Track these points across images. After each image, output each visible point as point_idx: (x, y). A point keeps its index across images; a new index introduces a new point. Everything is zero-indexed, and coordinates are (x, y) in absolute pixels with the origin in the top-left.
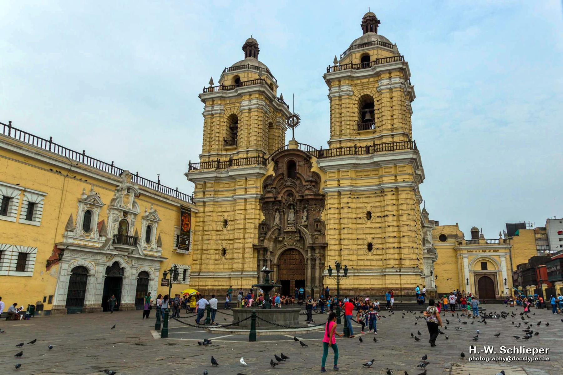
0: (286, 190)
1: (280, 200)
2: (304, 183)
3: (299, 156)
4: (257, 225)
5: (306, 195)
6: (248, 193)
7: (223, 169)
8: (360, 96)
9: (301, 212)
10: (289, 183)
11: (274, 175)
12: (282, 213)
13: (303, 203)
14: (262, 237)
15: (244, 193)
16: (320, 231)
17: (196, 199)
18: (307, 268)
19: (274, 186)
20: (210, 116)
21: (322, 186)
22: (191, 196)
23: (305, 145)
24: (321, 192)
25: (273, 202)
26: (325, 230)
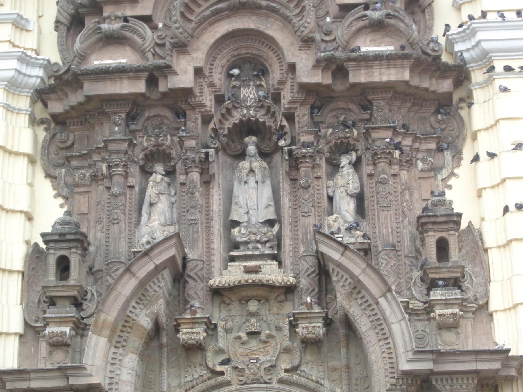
12: (195, 176)
13: (329, 119)
14: (62, 321)
26: (488, 280)
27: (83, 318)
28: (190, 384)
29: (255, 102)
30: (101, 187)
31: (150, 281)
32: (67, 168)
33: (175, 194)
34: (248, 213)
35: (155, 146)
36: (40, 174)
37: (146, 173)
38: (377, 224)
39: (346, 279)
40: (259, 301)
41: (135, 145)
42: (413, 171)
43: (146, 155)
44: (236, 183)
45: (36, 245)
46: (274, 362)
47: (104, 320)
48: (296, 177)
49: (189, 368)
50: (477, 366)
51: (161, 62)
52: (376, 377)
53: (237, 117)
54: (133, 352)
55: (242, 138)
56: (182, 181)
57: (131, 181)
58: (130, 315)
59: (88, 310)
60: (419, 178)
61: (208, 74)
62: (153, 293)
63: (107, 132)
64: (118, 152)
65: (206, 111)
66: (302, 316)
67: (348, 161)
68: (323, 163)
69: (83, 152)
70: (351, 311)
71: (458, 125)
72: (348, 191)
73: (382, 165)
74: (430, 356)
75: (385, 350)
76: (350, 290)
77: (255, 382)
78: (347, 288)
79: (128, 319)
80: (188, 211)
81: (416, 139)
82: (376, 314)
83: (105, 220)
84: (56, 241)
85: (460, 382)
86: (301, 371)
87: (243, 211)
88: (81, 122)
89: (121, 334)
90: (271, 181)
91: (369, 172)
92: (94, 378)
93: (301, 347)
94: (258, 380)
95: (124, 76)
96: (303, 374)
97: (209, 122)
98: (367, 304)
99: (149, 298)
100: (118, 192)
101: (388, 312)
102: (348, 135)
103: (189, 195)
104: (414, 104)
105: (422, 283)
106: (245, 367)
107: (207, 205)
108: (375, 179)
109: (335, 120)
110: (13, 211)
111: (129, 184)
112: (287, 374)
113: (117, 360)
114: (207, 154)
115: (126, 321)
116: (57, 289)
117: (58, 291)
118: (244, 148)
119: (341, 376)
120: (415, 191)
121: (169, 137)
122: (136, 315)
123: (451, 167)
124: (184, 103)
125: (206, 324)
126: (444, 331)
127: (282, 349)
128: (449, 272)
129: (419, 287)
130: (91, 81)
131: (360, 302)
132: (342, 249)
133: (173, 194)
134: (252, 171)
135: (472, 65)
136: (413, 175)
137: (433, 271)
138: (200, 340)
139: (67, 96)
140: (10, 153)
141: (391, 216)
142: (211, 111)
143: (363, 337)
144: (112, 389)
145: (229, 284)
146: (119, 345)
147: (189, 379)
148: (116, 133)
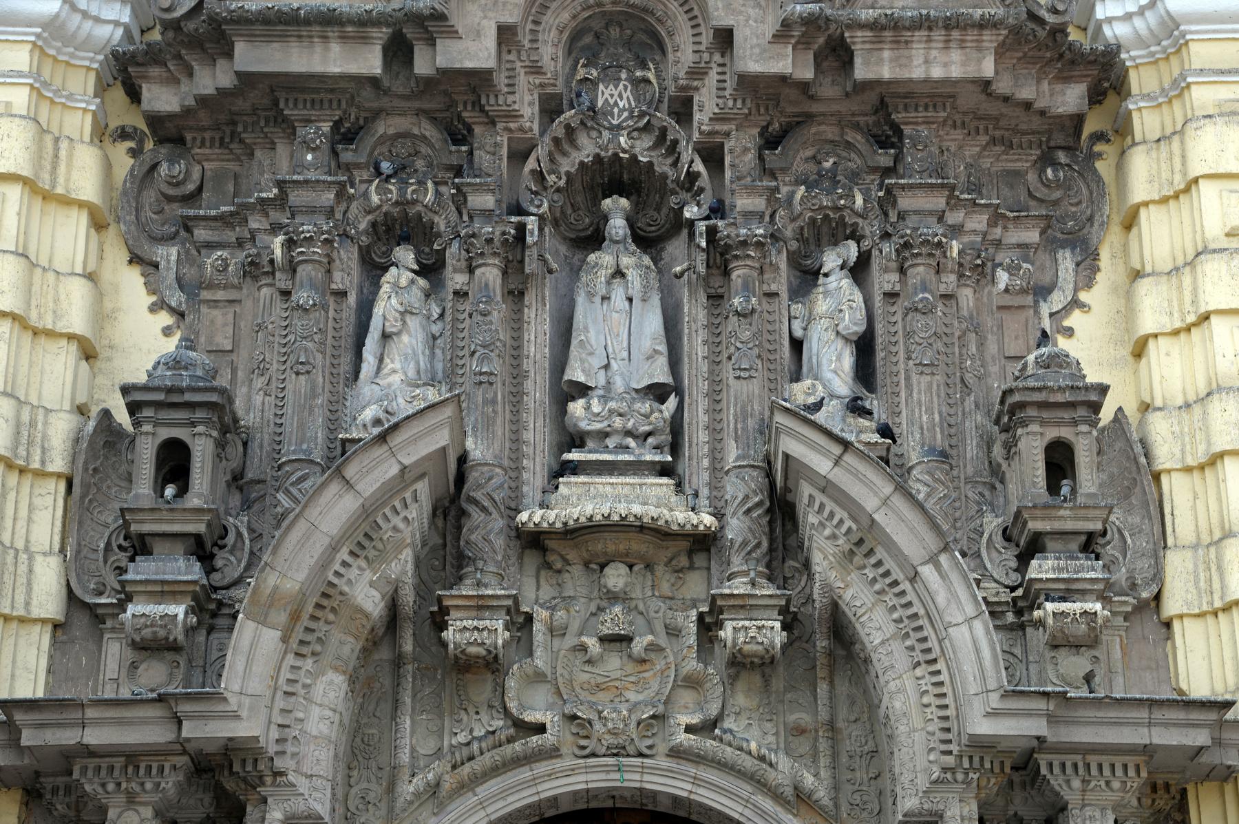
12: (490, 274)
13: (800, 165)
14: (165, 591)
27: (215, 589)
28: (465, 752)
29: (631, 117)
30: (265, 290)
31: (384, 504)
32: (183, 244)
33: (442, 316)
34: (607, 367)
35: (397, 203)
36: (117, 255)
38: (903, 406)
39: (841, 521)
40: (631, 567)
41: (351, 198)
42: (986, 291)
43: (374, 225)
44: (581, 299)
45: (106, 414)
46: (661, 708)
47: (276, 588)
48: (720, 291)
49: (463, 712)
50: (1150, 736)
52: (904, 750)
53: (587, 149)
54: (336, 669)
55: (596, 202)
56: (458, 287)
57: (340, 280)
58: (335, 581)
59: (226, 570)
60: (1000, 308)
61: (527, 45)
62: (390, 533)
63: (284, 164)
64: (312, 210)
65: (521, 129)
66: (732, 602)
67: (840, 262)
68: (782, 262)
69: (224, 209)
70: (848, 595)
71: (1091, 193)
72: (840, 328)
73: (919, 272)
74: (1041, 704)
75: (930, 688)
76: (847, 547)
77: (615, 751)
78: (840, 542)
79: (331, 591)
80: (473, 353)
81: (996, 218)
82: (909, 604)
83: (275, 366)
84: (158, 405)
85: (1107, 772)
86: (725, 731)
87: (597, 362)
88: (222, 139)
89: (313, 625)
90: (661, 299)
91: (888, 287)
92: (244, 724)
93: (725, 675)
94: (624, 748)
95: (333, 32)
96: (727, 737)
97: (526, 156)
98: (888, 581)
99: (380, 546)
100: (311, 302)
101: (941, 599)
102: (842, 202)
103: (477, 318)
104: (993, 141)
105: (1006, 544)
106: (593, 716)
107: (515, 344)
108: (903, 303)
109: (812, 167)
110: (50, 334)
111: (334, 286)
112: (692, 737)
113: (299, 686)
114: (521, 228)
115: (325, 595)
116: (157, 516)
117: (160, 521)
118: (598, 224)
119: (815, 747)
120: (990, 336)
121: (430, 184)
122: (349, 581)
123: (1071, 286)
124: (469, 108)
125: (508, 612)
126: (1063, 652)
127: (680, 678)
128: (1076, 518)
129: (1000, 553)
130: (251, 38)
131: (871, 576)
132: (837, 450)
133: (436, 316)
134: (619, 273)
135: (1133, 53)
136: (985, 299)
137: (1038, 513)
138: (496, 648)
139: (190, 74)
140: (47, 197)
141: (938, 386)
142: (531, 130)
143: (874, 657)
144: (284, 753)
145: (565, 524)
146: (304, 650)
147: (462, 738)
148: (305, 167)
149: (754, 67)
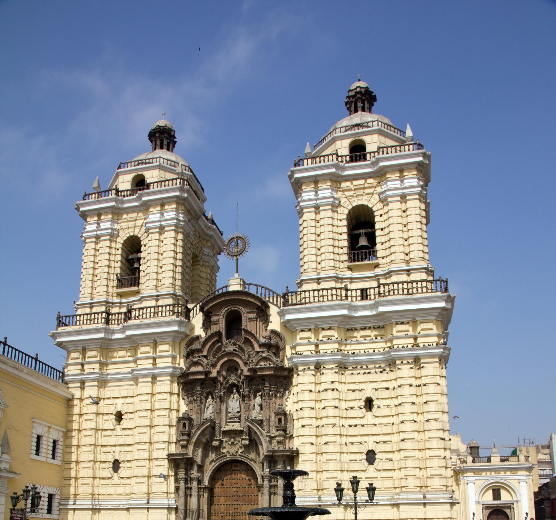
0: (226, 359)
1: (216, 378)
2: (257, 348)
3: (247, 304)
4: (174, 422)
5: (262, 369)
6: (158, 365)
7: (116, 326)
8: (350, 207)
9: (252, 398)
10: (231, 348)
11: (203, 335)
12: (218, 400)
15: (151, 366)
16: (285, 430)
17: (68, 375)
18: (262, 494)
19: (205, 353)
20: (94, 240)
21: (288, 352)
22: (61, 370)
23: (257, 286)
24: (286, 364)
25: (202, 382)
37: (207, 398)
51: (207, 370)
87: (231, 409)
134: (234, 398)
149: (245, 374)
